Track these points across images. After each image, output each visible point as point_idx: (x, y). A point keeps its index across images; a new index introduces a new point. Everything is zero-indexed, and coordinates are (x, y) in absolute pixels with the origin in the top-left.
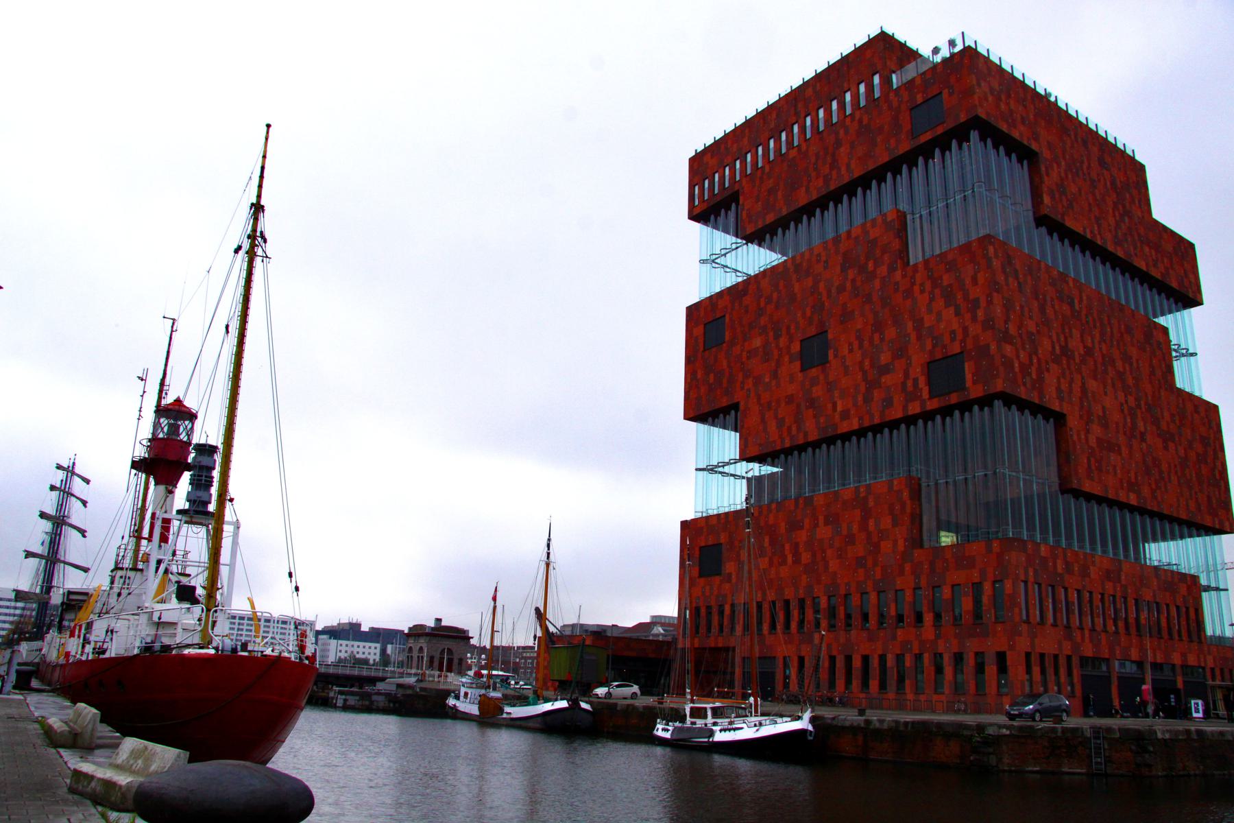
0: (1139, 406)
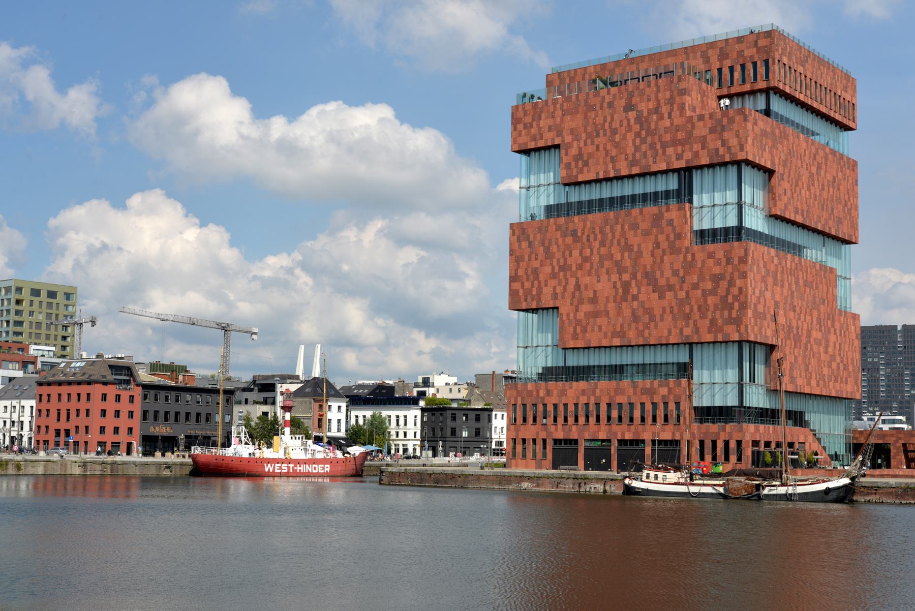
0: (634, 276)
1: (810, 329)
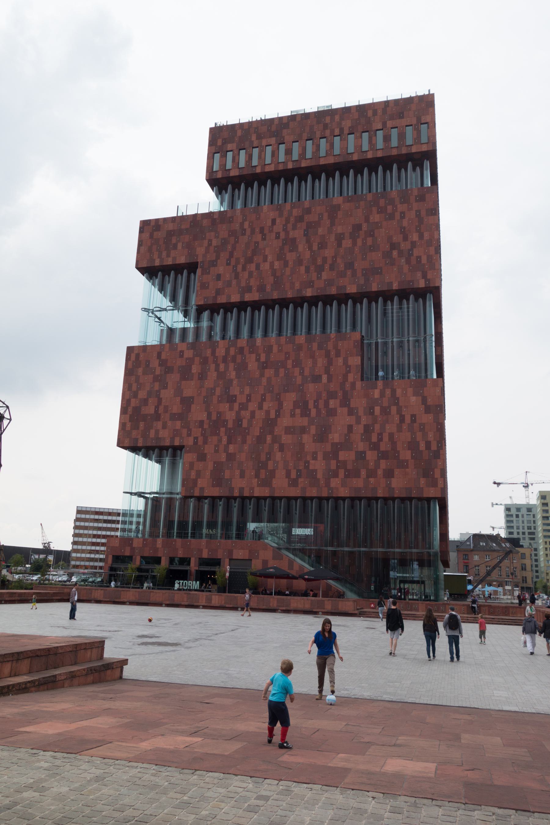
1: (273, 415)
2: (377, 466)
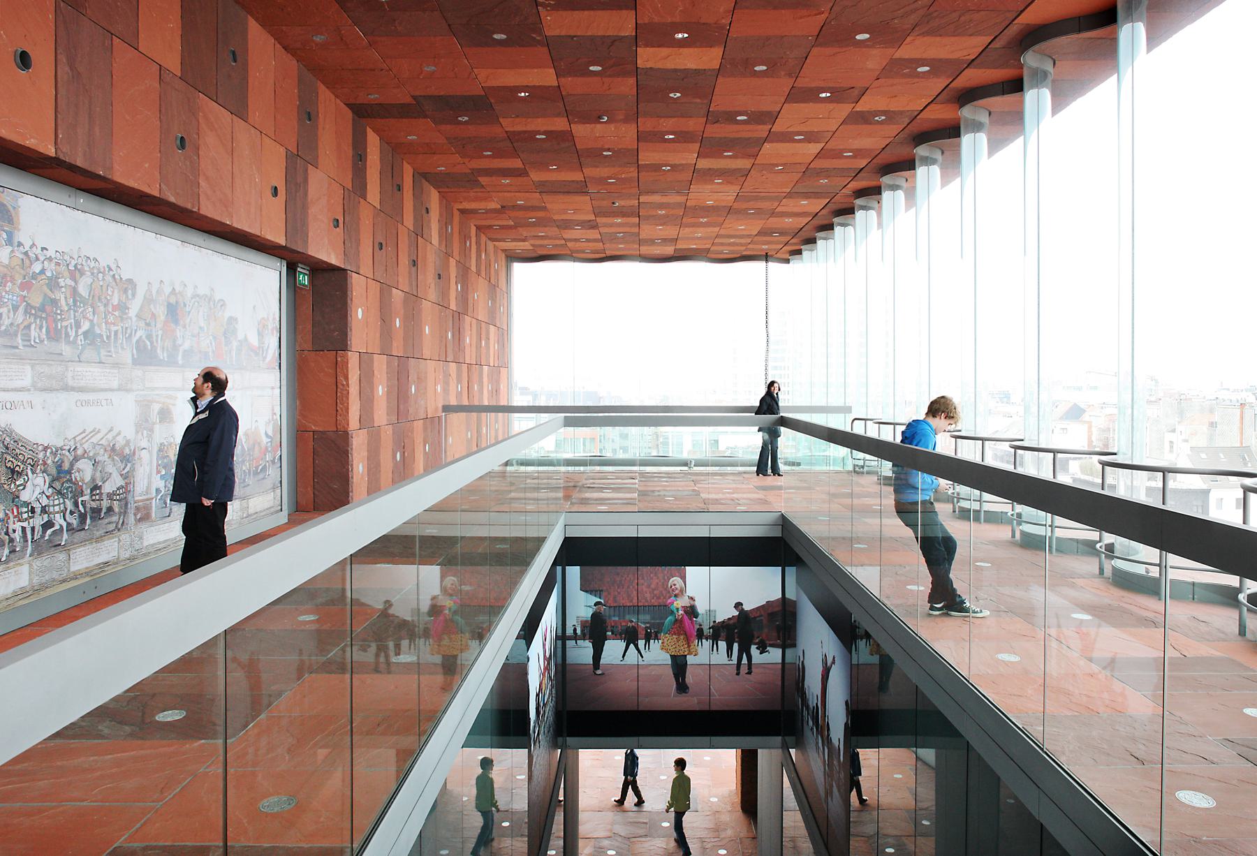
2: (666, 596)
